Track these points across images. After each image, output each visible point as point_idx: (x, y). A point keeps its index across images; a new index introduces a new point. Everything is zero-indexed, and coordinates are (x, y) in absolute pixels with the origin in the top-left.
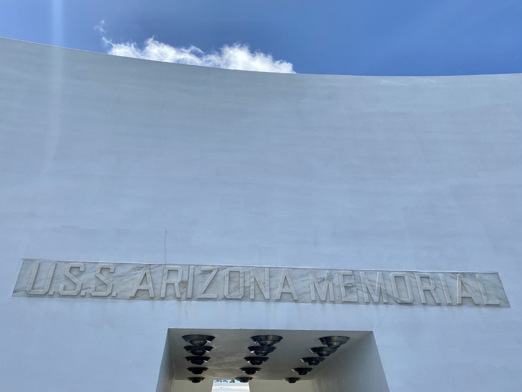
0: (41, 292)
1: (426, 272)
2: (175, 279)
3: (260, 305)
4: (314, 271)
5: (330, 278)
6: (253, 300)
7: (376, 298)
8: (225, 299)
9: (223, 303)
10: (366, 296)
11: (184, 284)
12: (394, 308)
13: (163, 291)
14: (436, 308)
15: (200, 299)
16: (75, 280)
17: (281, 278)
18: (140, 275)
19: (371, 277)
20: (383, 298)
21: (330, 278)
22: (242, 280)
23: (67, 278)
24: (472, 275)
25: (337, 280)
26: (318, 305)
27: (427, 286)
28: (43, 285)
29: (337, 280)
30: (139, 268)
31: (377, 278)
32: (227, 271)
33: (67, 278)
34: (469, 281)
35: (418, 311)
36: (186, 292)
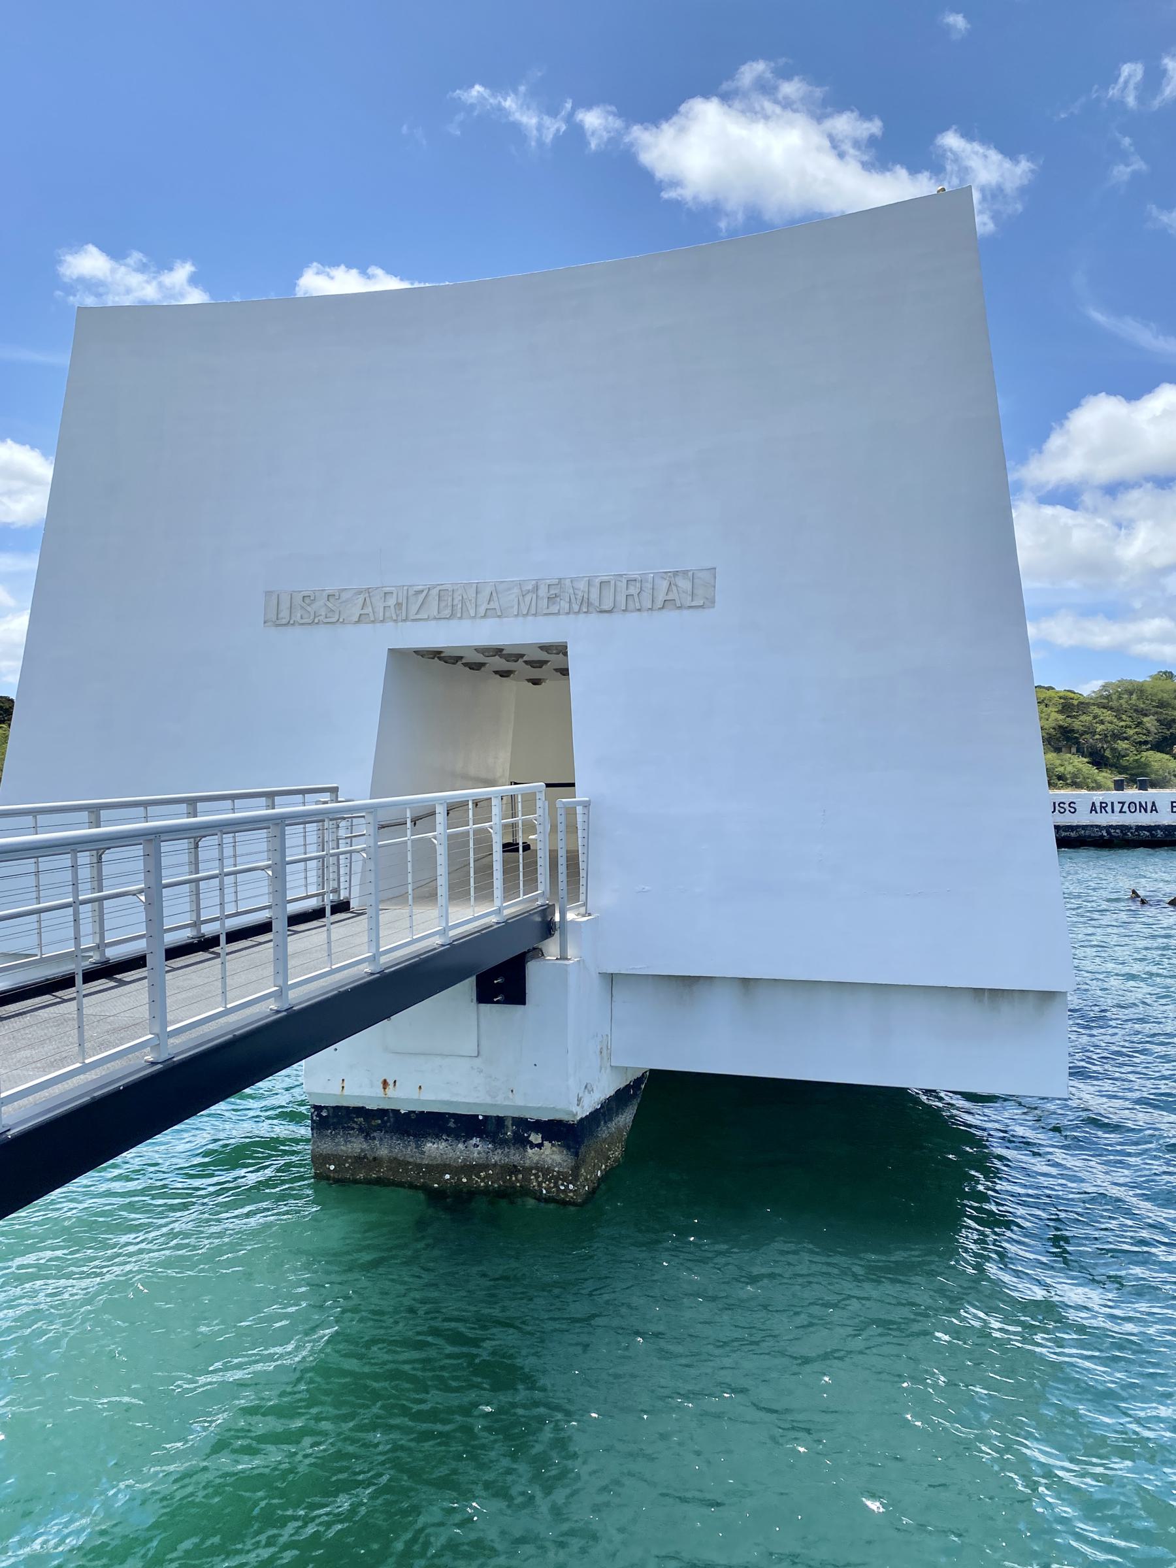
0: (284, 621)
1: (635, 574)
2: (392, 602)
3: (466, 623)
4: (520, 584)
5: (536, 588)
6: (461, 618)
7: (576, 608)
8: (435, 618)
9: (433, 622)
10: (567, 606)
11: (398, 605)
12: (594, 616)
13: (381, 614)
14: (638, 613)
15: (413, 620)
16: (309, 609)
17: (485, 595)
19: (576, 585)
20: (586, 606)
21: (536, 588)
22: (450, 599)
23: (302, 607)
24: (685, 572)
25: (543, 592)
26: (521, 619)
27: (633, 590)
28: (285, 614)
29: (543, 592)
30: (360, 592)
31: (582, 585)
32: (435, 592)
33: (302, 607)
35: (616, 617)
36: (401, 614)
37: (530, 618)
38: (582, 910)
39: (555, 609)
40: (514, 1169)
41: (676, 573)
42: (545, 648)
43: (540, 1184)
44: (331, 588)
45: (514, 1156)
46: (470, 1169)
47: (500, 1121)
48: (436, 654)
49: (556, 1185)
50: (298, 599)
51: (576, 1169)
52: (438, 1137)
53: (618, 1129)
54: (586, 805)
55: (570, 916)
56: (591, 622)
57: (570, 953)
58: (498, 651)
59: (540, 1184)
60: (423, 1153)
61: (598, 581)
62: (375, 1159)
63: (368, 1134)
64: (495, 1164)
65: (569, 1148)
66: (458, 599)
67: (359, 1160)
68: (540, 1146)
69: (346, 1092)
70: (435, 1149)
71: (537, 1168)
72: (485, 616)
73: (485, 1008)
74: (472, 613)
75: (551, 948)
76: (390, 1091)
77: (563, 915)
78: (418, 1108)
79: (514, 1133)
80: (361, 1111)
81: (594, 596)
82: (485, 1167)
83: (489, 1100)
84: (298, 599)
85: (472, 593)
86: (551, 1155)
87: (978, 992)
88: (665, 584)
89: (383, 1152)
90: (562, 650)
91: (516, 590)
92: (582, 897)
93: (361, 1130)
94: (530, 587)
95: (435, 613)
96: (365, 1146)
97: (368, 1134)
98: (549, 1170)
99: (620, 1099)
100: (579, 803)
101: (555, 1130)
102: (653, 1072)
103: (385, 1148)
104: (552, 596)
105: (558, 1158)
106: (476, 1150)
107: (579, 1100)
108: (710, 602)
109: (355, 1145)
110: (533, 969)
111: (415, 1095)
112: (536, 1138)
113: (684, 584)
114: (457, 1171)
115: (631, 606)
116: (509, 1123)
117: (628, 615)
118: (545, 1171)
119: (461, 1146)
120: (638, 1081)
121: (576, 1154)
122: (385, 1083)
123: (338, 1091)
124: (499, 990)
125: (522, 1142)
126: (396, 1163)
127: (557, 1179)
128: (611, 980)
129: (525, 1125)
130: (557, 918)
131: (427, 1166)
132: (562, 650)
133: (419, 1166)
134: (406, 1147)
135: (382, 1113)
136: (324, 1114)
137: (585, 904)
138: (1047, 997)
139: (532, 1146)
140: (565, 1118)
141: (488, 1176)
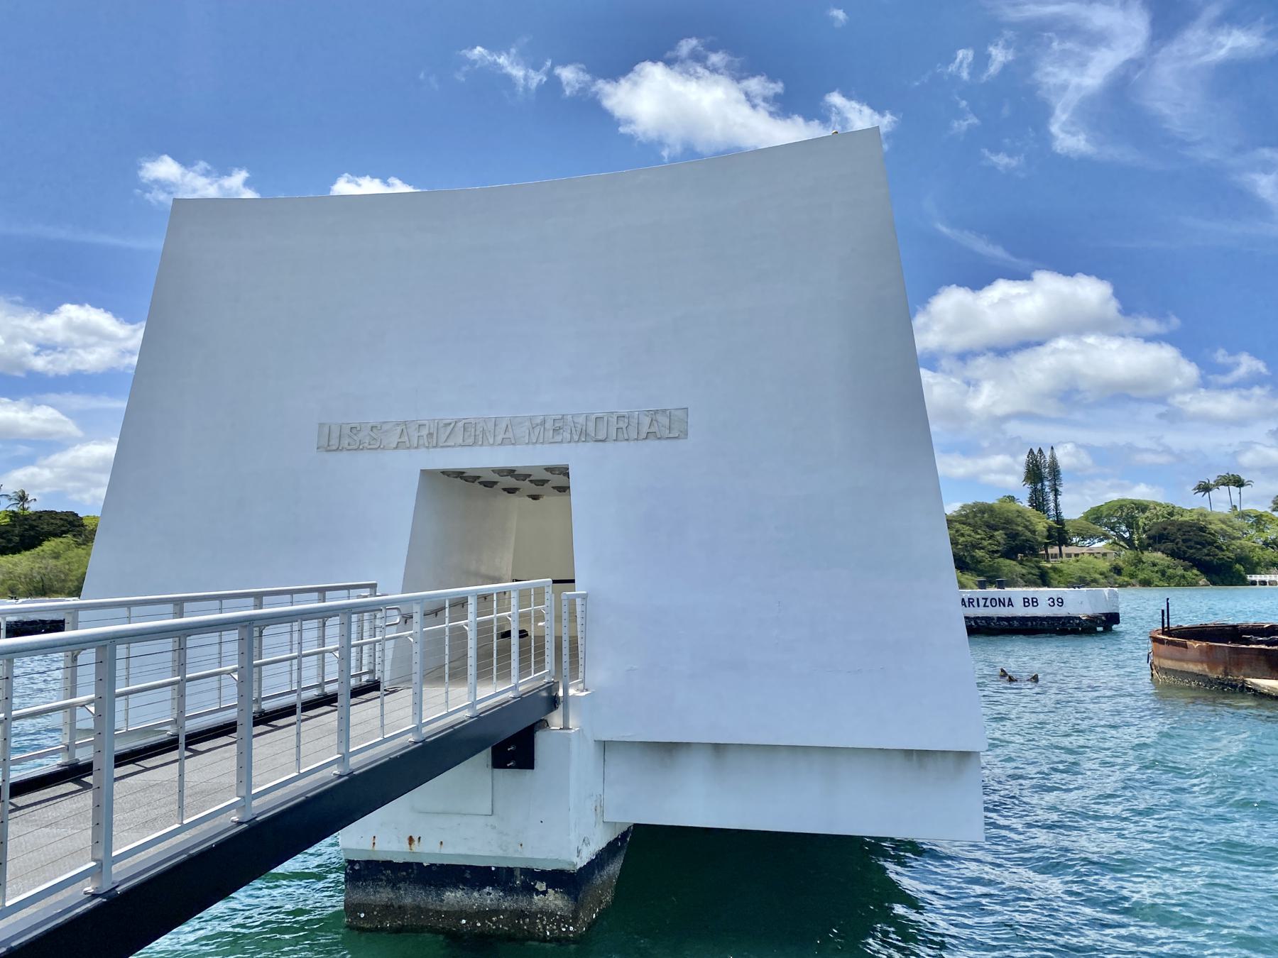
1: (623, 411)
4: (531, 418)
5: (544, 422)
7: (576, 438)
12: (590, 445)
18: (399, 429)
20: (584, 436)
21: (544, 422)
25: (549, 425)
27: (621, 424)
29: (549, 425)
31: (581, 420)
34: (659, 417)
35: (609, 446)
37: (538, 446)
38: (581, 686)
39: (558, 438)
40: (521, 914)
41: (656, 412)
42: (550, 469)
43: (544, 928)
44: (372, 420)
45: (522, 903)
46: (483, 914)
47: (510, 871)
48: (460, 474)
49: (558, 926)
50: (346, 430)
51: (575, 914)
52: (456, 887)
53: (609, 877)
54: (584, 597)
55: (572, 692)
56: (587, 448)
57: (571, 724)
58: (511, 472)
59: (544, 928)
60: (442, 901)
61: (593, 417)
62: (400, 907)
63: (394, 885)
64: (504, 912)
65: (569, 894)
66: (479, 429)
67: (387, 909)
68: (544, 893)
69: (377, 848)
70: (453, 897)
71: (541, 912)
72: (501, 444)
73: (500, 772)
74: (491, 441)
75: (556, 719)
76: (416, 847)
77: (566, 691)
78: (438, 862)
79: (523, 882)
80: (388, 864)
81: (591, 425)
82: (496, 912)
83: (500, 853)
84: (346, 430)
85: (491, 425)
86: (554, 900)
87: (908, 753)
88: (647, 421)
89: (408, 901)
90: (564, 471)
91: (528, 424)
92: (581, 675)
93: (389, 881)
94: (539, 421)
95: (460, 441)
96: (392, 895)
97: (394, 885)
98: (553, 914)
99: (610, 850)
100: (579, 596)
101: (558, 879)
102: (635, 825)
103: (410, 897)
104: (558, 428)
105: (559, 903)
106: (489, 897)
107: (579, 852)
108: (684, 434)
109: (383, 895)
110: (541, 738)
111: (436, 849)
112: (541, 886)
113: (665, 421)
114: (471, 916)
115: (620, 435)
116: (517, 873)
117: (619, 443)
118: (551, 914)
119: (476, 894)
120: (624, 835)
121: (576, 899)
122: (411, 840)
123: (370, 848)
124: (512, 756)
125: (530, 890)
126: (419, 910)
127: (559, 922)
128: (604, 746)
129: (532, 875)
130: (561, 693)
131: (445, 912)
132: (564, 471)
133: (438, 913)
134: (427, 896)
135: (407, 866)
136: (357, 867)
137: (583, 682)
138: (964, 756)
139: (538, 893)
140: (567, 867)
141: (499, 921)
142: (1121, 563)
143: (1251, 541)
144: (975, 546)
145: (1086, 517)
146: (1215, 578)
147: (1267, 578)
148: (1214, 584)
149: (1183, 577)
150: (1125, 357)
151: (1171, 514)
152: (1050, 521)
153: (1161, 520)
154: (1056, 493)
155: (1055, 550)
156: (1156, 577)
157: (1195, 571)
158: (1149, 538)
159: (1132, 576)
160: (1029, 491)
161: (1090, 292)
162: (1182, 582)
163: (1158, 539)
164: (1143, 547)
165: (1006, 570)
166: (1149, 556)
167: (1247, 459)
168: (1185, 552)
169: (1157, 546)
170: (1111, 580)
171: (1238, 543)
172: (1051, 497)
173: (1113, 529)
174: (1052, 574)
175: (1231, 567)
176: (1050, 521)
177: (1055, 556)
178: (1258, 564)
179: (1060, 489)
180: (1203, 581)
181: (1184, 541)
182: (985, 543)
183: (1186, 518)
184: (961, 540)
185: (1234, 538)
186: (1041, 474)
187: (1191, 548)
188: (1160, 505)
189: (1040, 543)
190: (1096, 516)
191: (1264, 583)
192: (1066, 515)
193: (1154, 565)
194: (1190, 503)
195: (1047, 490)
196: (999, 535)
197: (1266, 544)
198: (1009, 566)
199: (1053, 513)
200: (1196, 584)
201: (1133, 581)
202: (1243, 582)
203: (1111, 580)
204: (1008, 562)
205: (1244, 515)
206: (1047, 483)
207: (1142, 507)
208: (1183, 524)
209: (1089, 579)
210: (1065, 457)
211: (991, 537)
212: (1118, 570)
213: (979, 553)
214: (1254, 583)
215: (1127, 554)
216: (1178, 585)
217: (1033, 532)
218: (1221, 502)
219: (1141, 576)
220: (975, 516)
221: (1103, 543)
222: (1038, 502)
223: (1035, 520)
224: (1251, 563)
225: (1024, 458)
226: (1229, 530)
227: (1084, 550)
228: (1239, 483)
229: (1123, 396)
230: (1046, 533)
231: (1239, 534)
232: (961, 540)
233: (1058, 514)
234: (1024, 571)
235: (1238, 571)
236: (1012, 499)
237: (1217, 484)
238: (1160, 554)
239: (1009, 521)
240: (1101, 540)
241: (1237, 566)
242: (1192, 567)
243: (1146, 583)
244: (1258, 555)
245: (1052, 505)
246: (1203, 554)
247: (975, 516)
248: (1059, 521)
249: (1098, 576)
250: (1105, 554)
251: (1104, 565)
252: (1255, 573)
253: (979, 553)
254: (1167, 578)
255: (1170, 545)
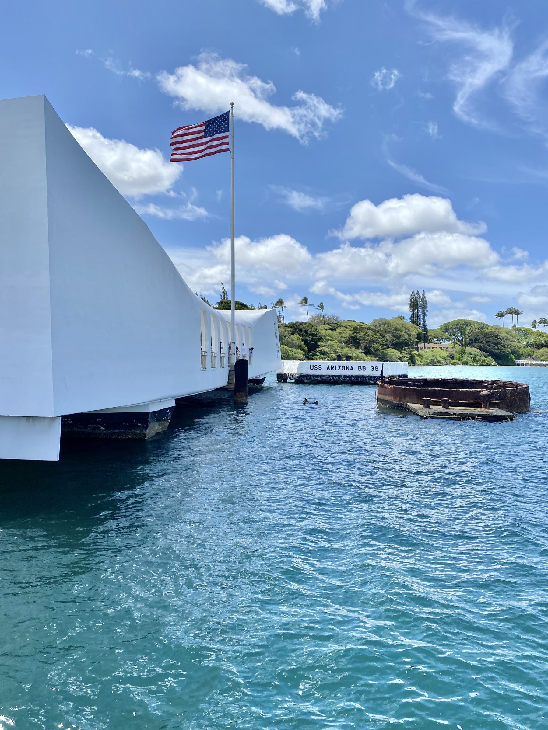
142: (454, 353)
143: (520, 344)
144: (374, 342)
145: (441, 329)
146: (500, 362)
147: (524, 362)
148: (499, 364)
149: (484, 361)
150: (461, 244)
151: (482, 328)
152: (421, 330)
153: (477, 331)
154: (424, 315)
155: (421, 345)
156: (470, 361)
157: (490, 358)
158: (470, 340)
159: (459, 360)
160: (411, 313)
161: (440, 207)
162: (484, 363)
163: (474, 341)
164: (466, 345)
165: (391, 354)
166: (468, 349)
167: (521, 301)
168: (487, 348)
169: (473, 344)
170: (448, 361)
171: (513, 344)
172: (422, 317)
173: (454, 335)
174: (417, 358)
175: (508, 356)
176: (421, 330)
177: (422, 348)
178: (522, 355)
179: (427, 313)
180: (494, 363)
181: (487, 342)
182: (380, 340)
183: (489, 330)
184: (367, 338)
185: (512, 341)
186: (417, 305)
187: (489, 346)
188: (477, 323)
189: (413, 341)
190: (446, 329)
191: (523, 365)
192: (428, 327)
193: (471, 354)
194: (490, 321)
195: (420, 313)
196: (389, 336)
197: (528, 345)
198: (392, 352)
199: (422, 325)
200: (489, 364)
201: (459, 362)
202: (512, 363)
203: (448, 361)
204: (393, 350)
205: (518, 330)
206: (420, 310)
207: (467, 323)
208: (486, 333)
209: (436, 360)
210: (431, 297)
211: (383, 337)
212: (452, 357)
213: (376, 345)
214: (518, 365)
215: (459, 348)
216: (481, 365)
217: (410, 335)
218: (509, 322)
219: (464, 360)
220: (380, 326)
221: (449, 342)
222: (415, 320)
223: (411, 329)
224: (519, 355)
225: (409, 297)
226: (509, 337)
227: (437, 345)
228: (517, 313)
229: (461, 266)
230: (416, 336)
231: (513, 339)
232: (367, 338)
233: (425, 327)
234: (401, 356)
235: (511, 358)
236: (402, 318)
237: (507, 313)
238: (474, 349)
239: (397, 329)
240: (448, 341)
241: (512, 356)
242: (489, 356)
243: (466, 363)
244: (523, 350)
245: (422, 322)
246: (495, 349)
247: (380, 326)
248: (425, 330)
249: (440, 359)
250: (447, 348)
251: (445, 354)
252: (519, 360)
253: (376, 345)
254: (476, 361)
255: (479, 344)
